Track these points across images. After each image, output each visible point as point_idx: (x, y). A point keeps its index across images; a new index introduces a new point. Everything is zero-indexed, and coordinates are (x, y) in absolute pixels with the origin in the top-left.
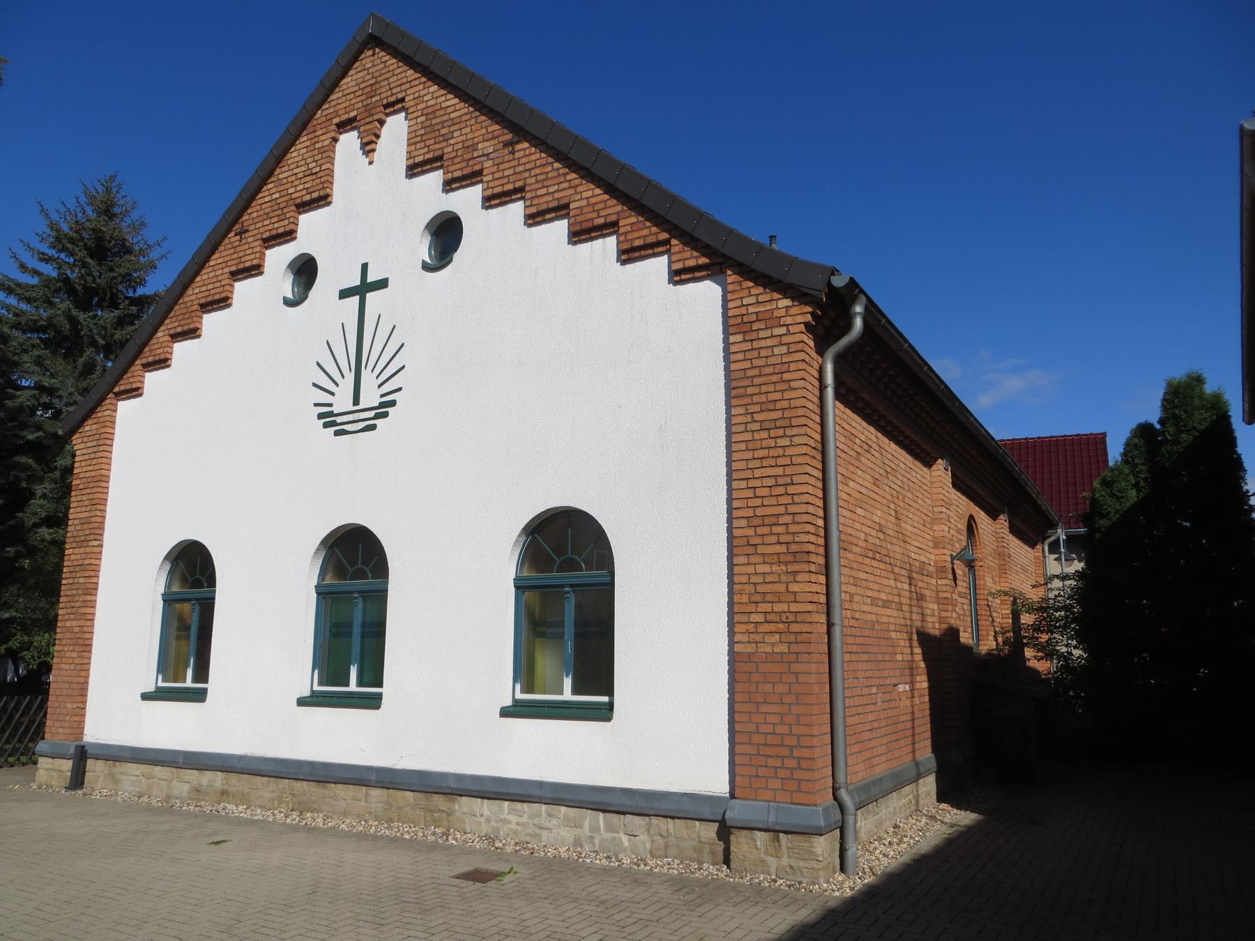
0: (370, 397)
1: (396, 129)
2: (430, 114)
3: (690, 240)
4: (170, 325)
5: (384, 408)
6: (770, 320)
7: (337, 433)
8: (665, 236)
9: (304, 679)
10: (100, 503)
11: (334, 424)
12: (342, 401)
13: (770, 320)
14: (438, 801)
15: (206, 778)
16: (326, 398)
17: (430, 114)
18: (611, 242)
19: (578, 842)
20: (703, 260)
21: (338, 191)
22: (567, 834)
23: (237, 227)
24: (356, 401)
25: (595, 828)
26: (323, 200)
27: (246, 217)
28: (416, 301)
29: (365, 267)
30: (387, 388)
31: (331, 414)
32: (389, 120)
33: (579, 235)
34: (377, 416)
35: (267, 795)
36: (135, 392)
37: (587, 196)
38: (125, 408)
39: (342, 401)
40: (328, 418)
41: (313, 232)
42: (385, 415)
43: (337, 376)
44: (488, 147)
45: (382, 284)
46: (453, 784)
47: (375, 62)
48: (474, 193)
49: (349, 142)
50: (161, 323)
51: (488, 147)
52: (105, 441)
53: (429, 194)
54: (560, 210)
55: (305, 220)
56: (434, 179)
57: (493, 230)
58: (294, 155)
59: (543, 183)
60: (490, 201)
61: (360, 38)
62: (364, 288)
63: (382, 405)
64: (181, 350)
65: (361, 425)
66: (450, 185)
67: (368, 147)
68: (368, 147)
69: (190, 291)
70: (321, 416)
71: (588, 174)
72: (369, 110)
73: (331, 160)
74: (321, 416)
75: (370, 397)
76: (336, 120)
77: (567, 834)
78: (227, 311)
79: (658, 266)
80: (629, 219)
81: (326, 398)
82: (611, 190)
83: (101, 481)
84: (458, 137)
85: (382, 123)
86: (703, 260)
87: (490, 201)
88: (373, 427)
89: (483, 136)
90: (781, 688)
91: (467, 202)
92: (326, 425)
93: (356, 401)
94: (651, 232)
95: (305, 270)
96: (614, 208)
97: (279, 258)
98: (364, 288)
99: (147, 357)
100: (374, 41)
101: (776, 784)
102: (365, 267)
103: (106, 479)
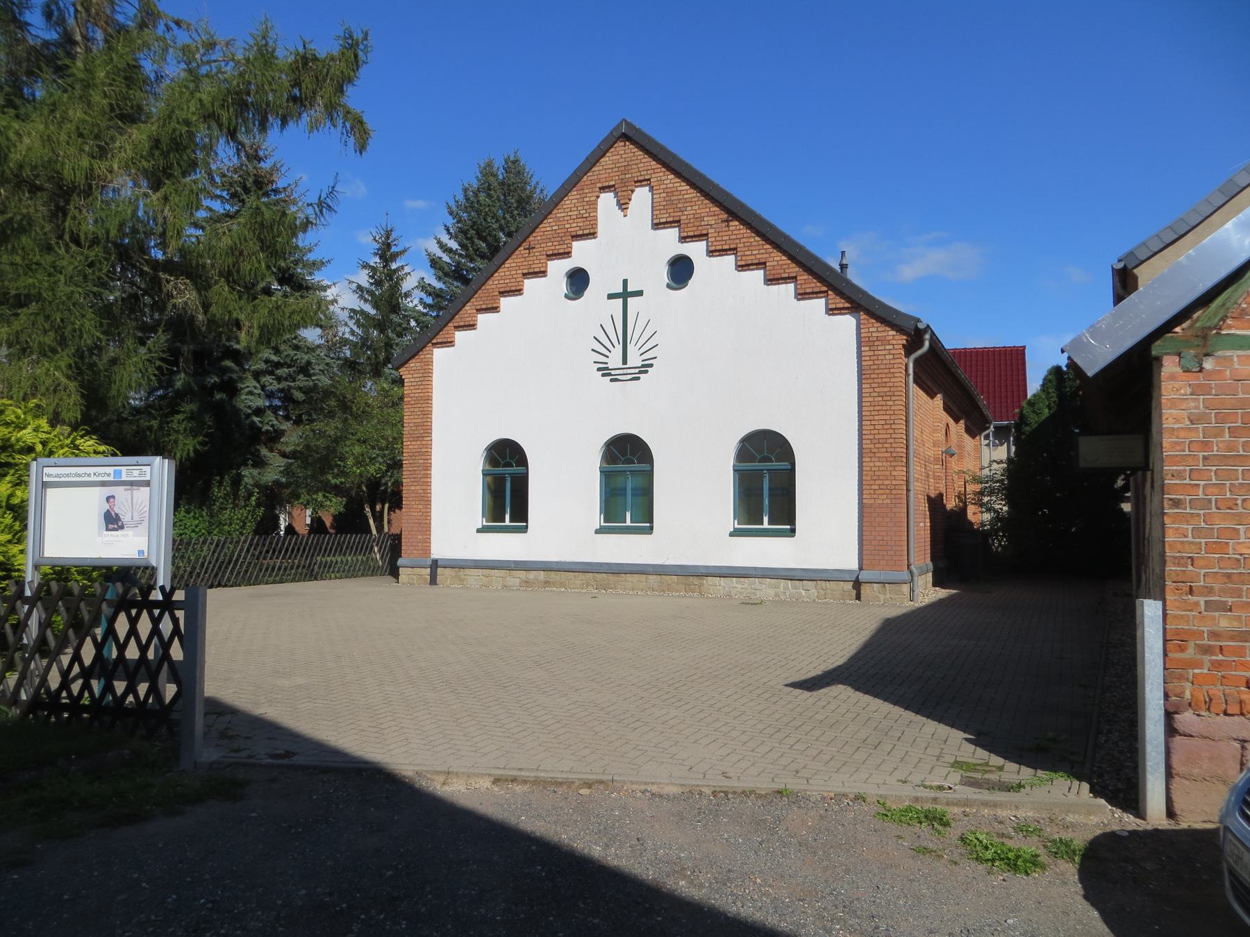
0: (635, 360)
1: (642, 196)
2: (670, 193)
3: (840, 293)
4: (475, 302)
5: (645, 368)
6: (884, 341)
7: (612, 380)
8: (825, 289)
9: (597, 520)
10: (427, 414)
11: (610, 375)
12: (615, 361)
13: (884, 341)
14: (696, 580)
15: (532, 575)
16: (603, 359)
17: (670, 193)
18: (791, 286)
19: (777, 595)
20: (847, 305)
21: (600, 230)
22: (771, 592)
23: (525, 245)
24: (625, 362)
25: (786, 588)
26: (592, 235)
27: (531, 238)
28: (657, 303)
29: (625, 282)
30: (645, 357)
31: (607, 369)
32: (637, 190)
33: (771, 280)
34: (640, 372)
35: (578, 582)
36: (449, 343)
37: (777, 260)
38: (439, 355)
39: (615, 361)
40: (605, 371)
41: (582, 254)
42: (646, 372)
43: (610, 347)
44: (711, 220)
45: (639, 293)
46: (704, 571)
47: (624, 151)
48: (701, 246)
49: (607, 201)
50: (468, 301)
51: (711, 220)
52: (426, 374)
53: (669, 243)
54: (761, 265)
55: (577, 246)
56: (673, 233)
57: (714, 272)
58: (567, 202)
59: (749, 247)
60: (711, 253)
61: (616, 134)
62: (625, 295)
63: (643, 366)
64: (482, 318)
65: (629, 377)
66: (683, 239)
67: (623, 205)
68: (623, 205)
69: (490, 282)
70: (599, 369)
71: (777, 247)
72: (624, 183)
73: (595, 210)
74: (599, 369)
75: (635, 360)
76: (599, 185)
77: (771, 592)
78: (519, 297)
79: (820, 303)
80: (804, 277)
81: (603, 359)
82: (792, 258)
83: (426, 400)
84: (689, 211)
85: (633, 191)
86: (847, 305)
87: (711, 253)
88: (638, 378)
89: (711, 215)
90: (887, 520)
91: (696, 251)
92: (603, 375)
93: (625, 362)
94: (816, 285)
95: (578, 281)
96: (794, 269)
97: (558, 269)
98: (625, 295)
99: (458, 320)
100: (626, 137)
101: (883, 562)
102: (625, 282)
103: (429, 398)
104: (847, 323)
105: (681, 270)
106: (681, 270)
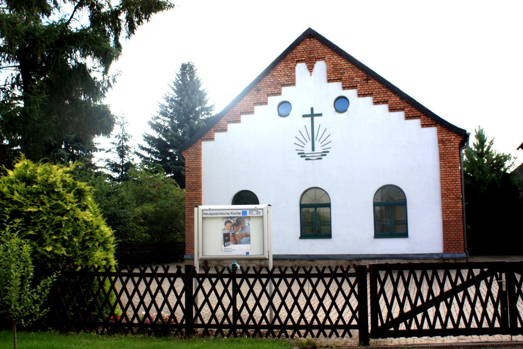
0: (319, 149)
2: (335, 65)
5: (324, 153)
6: (450, 141)
7: (306, 159)
11: (305, 156)
12: (307, 149)
13: (450, 141)
16: (302, 149)
17: (335, 65)
24: (313, 149)
29: (312, 109)
30: (324, 147)
31: (303, 153)
34: (322, 155)
37: (395, 99)
39: (307, 149)
40: (302, 155)
42: (325, 155)
52: (198, 155)
53: (336, 89)
54: (385, 102)
55: (284, 89)
59: (379, 93)
60: (361, 95)
62: (312, 115)
63: (323, 152)
65: (316, 158)
70: (299, 154)
74: (299, 154)
75: (319, 149)
84: (346, 74)
88: (321, 159)
90: (455, 228)
91: (351, 94)
92: (301, 157)
93: (313, 149)
97: (274, 101)
101: (454, 249)
102: (312, 109)
104: (432, 132)
105: (341, 104)
106: (341, 104)
